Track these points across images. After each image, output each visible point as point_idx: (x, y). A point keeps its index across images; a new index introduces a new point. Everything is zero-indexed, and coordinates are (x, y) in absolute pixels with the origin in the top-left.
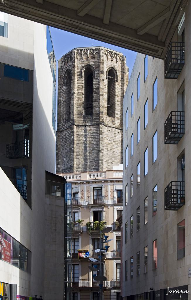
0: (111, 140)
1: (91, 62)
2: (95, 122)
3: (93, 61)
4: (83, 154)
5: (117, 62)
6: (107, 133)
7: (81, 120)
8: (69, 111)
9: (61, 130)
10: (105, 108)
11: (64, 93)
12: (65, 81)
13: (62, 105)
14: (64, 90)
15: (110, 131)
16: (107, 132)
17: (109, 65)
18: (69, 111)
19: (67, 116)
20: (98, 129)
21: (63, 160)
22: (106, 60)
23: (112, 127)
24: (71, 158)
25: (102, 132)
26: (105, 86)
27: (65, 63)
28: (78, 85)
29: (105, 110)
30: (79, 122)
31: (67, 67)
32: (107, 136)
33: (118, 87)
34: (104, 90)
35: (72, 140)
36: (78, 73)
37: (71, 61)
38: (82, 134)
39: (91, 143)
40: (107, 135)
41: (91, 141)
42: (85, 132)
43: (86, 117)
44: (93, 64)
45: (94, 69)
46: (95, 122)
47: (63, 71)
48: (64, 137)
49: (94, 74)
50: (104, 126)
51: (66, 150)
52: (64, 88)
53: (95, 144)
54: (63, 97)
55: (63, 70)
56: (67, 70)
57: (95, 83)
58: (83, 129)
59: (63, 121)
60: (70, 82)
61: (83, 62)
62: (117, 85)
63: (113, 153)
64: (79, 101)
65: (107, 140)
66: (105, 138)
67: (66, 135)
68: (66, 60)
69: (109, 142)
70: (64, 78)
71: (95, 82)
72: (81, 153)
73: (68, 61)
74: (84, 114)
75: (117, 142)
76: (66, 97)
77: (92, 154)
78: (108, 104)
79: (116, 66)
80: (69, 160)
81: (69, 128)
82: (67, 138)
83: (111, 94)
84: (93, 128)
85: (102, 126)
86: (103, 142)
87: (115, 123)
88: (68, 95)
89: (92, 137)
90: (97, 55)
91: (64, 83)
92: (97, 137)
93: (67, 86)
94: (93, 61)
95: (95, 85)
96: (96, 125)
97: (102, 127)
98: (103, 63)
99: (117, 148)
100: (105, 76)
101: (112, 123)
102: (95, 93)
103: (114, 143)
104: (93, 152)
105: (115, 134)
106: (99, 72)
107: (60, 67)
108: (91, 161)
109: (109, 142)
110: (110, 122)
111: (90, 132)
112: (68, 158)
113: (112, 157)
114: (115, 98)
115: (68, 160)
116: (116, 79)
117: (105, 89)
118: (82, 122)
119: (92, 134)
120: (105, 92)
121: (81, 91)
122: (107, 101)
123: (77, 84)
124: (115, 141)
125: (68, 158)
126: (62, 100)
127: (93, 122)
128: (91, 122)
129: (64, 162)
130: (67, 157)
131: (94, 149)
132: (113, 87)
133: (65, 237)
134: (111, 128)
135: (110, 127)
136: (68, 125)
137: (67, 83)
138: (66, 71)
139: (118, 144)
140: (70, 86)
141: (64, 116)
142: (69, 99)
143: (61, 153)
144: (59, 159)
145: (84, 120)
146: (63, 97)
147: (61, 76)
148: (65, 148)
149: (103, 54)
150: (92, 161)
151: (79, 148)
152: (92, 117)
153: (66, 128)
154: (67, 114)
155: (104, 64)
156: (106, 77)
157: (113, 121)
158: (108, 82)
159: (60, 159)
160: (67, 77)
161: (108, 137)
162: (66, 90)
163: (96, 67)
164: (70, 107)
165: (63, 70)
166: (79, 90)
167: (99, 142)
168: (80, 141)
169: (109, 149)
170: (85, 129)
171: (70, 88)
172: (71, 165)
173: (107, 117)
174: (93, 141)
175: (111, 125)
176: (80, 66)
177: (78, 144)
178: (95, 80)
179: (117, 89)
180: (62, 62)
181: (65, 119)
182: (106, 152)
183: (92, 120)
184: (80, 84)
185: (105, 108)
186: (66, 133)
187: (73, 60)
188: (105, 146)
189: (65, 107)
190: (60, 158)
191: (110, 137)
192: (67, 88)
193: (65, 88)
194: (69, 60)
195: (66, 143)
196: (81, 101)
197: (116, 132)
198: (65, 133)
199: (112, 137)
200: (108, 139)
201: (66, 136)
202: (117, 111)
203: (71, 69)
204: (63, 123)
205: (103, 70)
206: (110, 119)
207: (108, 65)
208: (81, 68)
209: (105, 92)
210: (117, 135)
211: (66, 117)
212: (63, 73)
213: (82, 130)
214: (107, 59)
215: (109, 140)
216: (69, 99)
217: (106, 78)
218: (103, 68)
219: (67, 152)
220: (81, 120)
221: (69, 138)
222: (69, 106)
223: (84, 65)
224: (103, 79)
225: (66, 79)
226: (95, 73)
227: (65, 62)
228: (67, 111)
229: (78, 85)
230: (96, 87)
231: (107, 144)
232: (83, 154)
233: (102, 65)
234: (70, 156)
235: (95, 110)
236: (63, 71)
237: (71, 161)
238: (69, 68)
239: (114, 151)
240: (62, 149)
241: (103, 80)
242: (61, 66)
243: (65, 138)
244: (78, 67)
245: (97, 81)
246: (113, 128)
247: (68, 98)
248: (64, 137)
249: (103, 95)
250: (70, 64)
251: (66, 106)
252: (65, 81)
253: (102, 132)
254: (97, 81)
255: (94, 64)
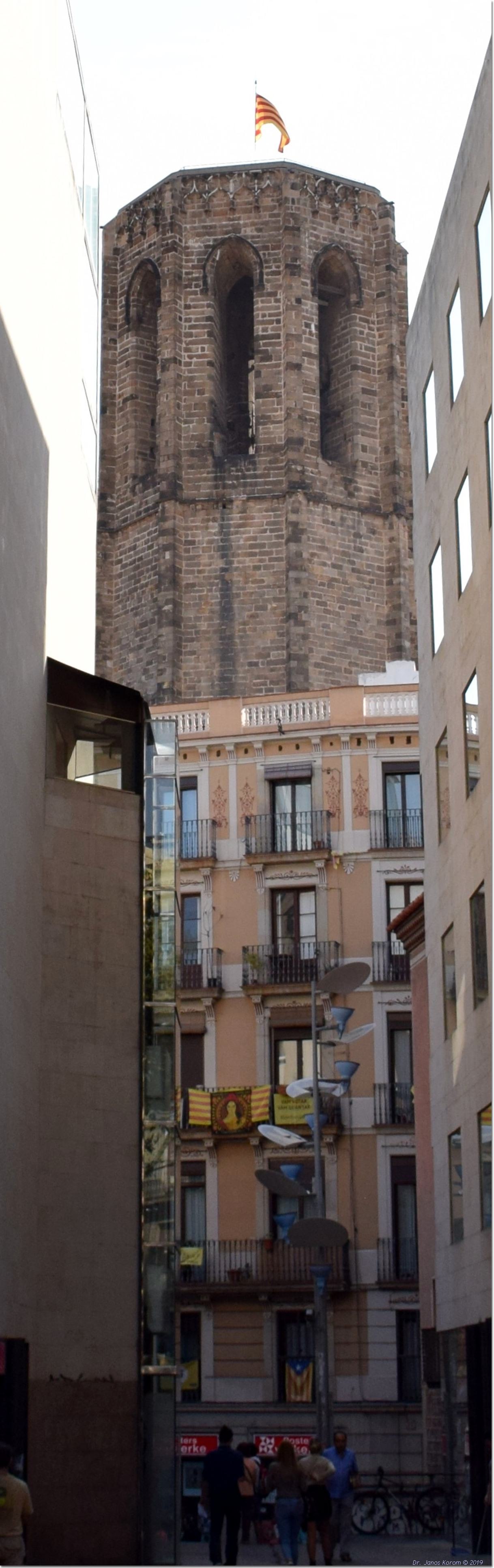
0: (339, 567)
1: (245, 225)
2: (266, 483)
3: (253, 224)
4: (215, 632)
5: (355, 224)
6: (322, 532)
7: (205, 479)
8: (149, 439)
9: (115, 524)
10: (311, 420)
11: (127, 364)
12: (133, 311)
13: (118, 415)
14: (127, 350)
15: (333, 523)
16: (322, 531)
17: (325, 239)
18: (149, 439)
19: (140, 461)
20: (280, 516)
21: (125, 660)
22: (309, 217)
23: (341, 506)
24: (160, 652)
25: (300, 527)
26: (308, 326)
27: (130, 237)
28: (191, 327)
29: (312, 430)
30: (198, 488)
31: (139, 253)
32: (323, 548)
33: (366, 331)
34: (303, 343)
35: (163, 568)
36: (187, 273)
37: (157, 225)
38: (210, 542)
39: (253, 582)
40: (322, 541)
41: (250, 572)
42: (224, 531)
43: (227, 466)
44: (253, 237)
45: (258, 256)
46: (266, 483)
47: (122, 269)
48: (130, 556)
49: (257, 277)
50: (309, 500)
51: (136, 615)
52: (130, 341)
53: (268, 587)
54: (125, 380)
55: (122, 263)
56: (143, 263)
57: (264, 316)
58: (214, 520)
59: (122, 485)
60: (156, 311)
61: (211, 227)
62: (361, 319)
63: (349, 623)
64: (191, 393)
65: (324, 564)
66: (313, 555)
67: (135, 547)
68: (134, 225)
69: (334, 573)
70: (127, 300)
71: (262, 309)
72: (204, 626)
73: (143, 225)
74: (218, 449)
75: (369, 573)
76: (139, 381)
77: (255, 630)
78: (324, 402)
79: (353, 240)
80: (149, 663)
81: (150, 515)
82: (141, 559)
83: (334, 362)
84: (260, 511)
85: (300, 502)
86: (304, 575)
87: (357, 489)
88: (144, 371)
89: (254, 554)
90: (268, 196)
91: (127, 319)
92: (278, 552)
93: (142, 333)
94: (253, 224)
95: (263, 322)
96: (274, 497)
97: (297, 505)
98: (298, 229)
99: (368, 599)
100: (305, 284)
101: (342, 488)
102: (262, 360)
103: (353, 579)
104: (262, 623)
105: (358, 535)
106: (278, 267)
107: (111, 254)
108: (251, 664)
109: (334, 573)
110: (335, 483)
111: (244, 533)
112: (148, 650)
113: (349, 644)
114: (350, 376)
115: (145, 661)
116: (353, 298)
117: (309, 340)
118: (210, 487)
119: (255, 538)
120: (309, 355)
121: (203, 349)
122: (318, 391)
123: (187, 320)
124: (358, 571)
125: (148, 650)
126: (118, 393)
127: (256, 484)
128: (251, 485)
129: (130, 671)
130: (140, 647)
131: (264, 608)
132: (343, 329)
133: (148, 1004)
134: (339, 509)
135: (335, 506)
136: (147, 503)
137: (140, 320)
138: (138, 268)
139: (372, 581)
140: (156, 332)
141: (127, 465)
142: (150, 386)
143: (116, 629)
144: (106, 658)
145: (216, 479)
146: (125, 380)
147: (114, 290)
148: (130, 604)
149: (295, 194)
150: (256, 664)
151: (195, 605)
152: (254, 463)
153: (139, 514)
154: (139, 453)
155: (303, 236)
156: (309, 287)
157: (348, 482)
158: (321, 309)
159: (110, 658)
160: (139, 293)
161: (325, 553)
162: (137, 347)
163: (266, 248)
164: (153, 422)
165: (122, 263)
166: (194, 347)
167: (287, 577)
168: (200, 572)
169: (334, 606)
170: (223, 519)
171: (155, 339)
172: (160, 685)
173: (320, 460)
174: (258, 572)
175: (338, 496)
176: (196, 245)
177: (193, 585)
178: (262, 302)
179: (363, 340)
180: (120, 232)
181: (135, 477)
182: (320, 618)
183: (255, 476)
184: (197, 320)
185: (311, 420)
186: (138, 539)
187: (166, 219)
188: (314, 595)
189: (132, 422)
190: (111, 652)
191: (336, 552)
192: (142, 342)
193: (128, 343)
194: (150, 221)
195: (139, 581)
196: (201, 392)
197: (363, 530)
198: (131, 539)
199: (344, 554)
200: (329, 563)
201: (136, 554)
202: (363, 434)
203: (158, 259)
204: (125, 493)
205: (296, 260)
206: (334, 471)
207: (317, 237)
208: (199, 254)
209: (309, 355)
210: (366, 544)
211: (136, 465)
212: (122, 279)
213: (208, 520)
214: (315, 213)
215: (334, 566)
216: (150, 386)
217: (313, 294)
218: (297, 249)
219: (143, 625)
220: (205, 479)
221: (150, 562)
222: (150, 417)
223: (215, 240)
224: (299, 293)
225: (138, 300)
226: (261, 274)
227: (130, 230)
228: (143, 442)
229: (191, 327)
230: (270, 332)
231: (322, 584)
232: (215, 632)
233: (294, 235)
234: (155, 641)
235: (265, 433)
236: (122, 269)
237: (161, 667)
238: (151, 252)
239: (357, 617)
240: (118, 609)
241: (298, 301)
242: (116, 251)
243: (134, 561)
244: (187, 248)
245: (273, 304)
246: (351, 508)
247: (145, 385)
248: (130, 556)
249: (298, 367)
250: (154, 237)
251: (136, 418)
252: (133, 311)
253: (300, 527)
254: (273, 304)
255: (258, 237)
